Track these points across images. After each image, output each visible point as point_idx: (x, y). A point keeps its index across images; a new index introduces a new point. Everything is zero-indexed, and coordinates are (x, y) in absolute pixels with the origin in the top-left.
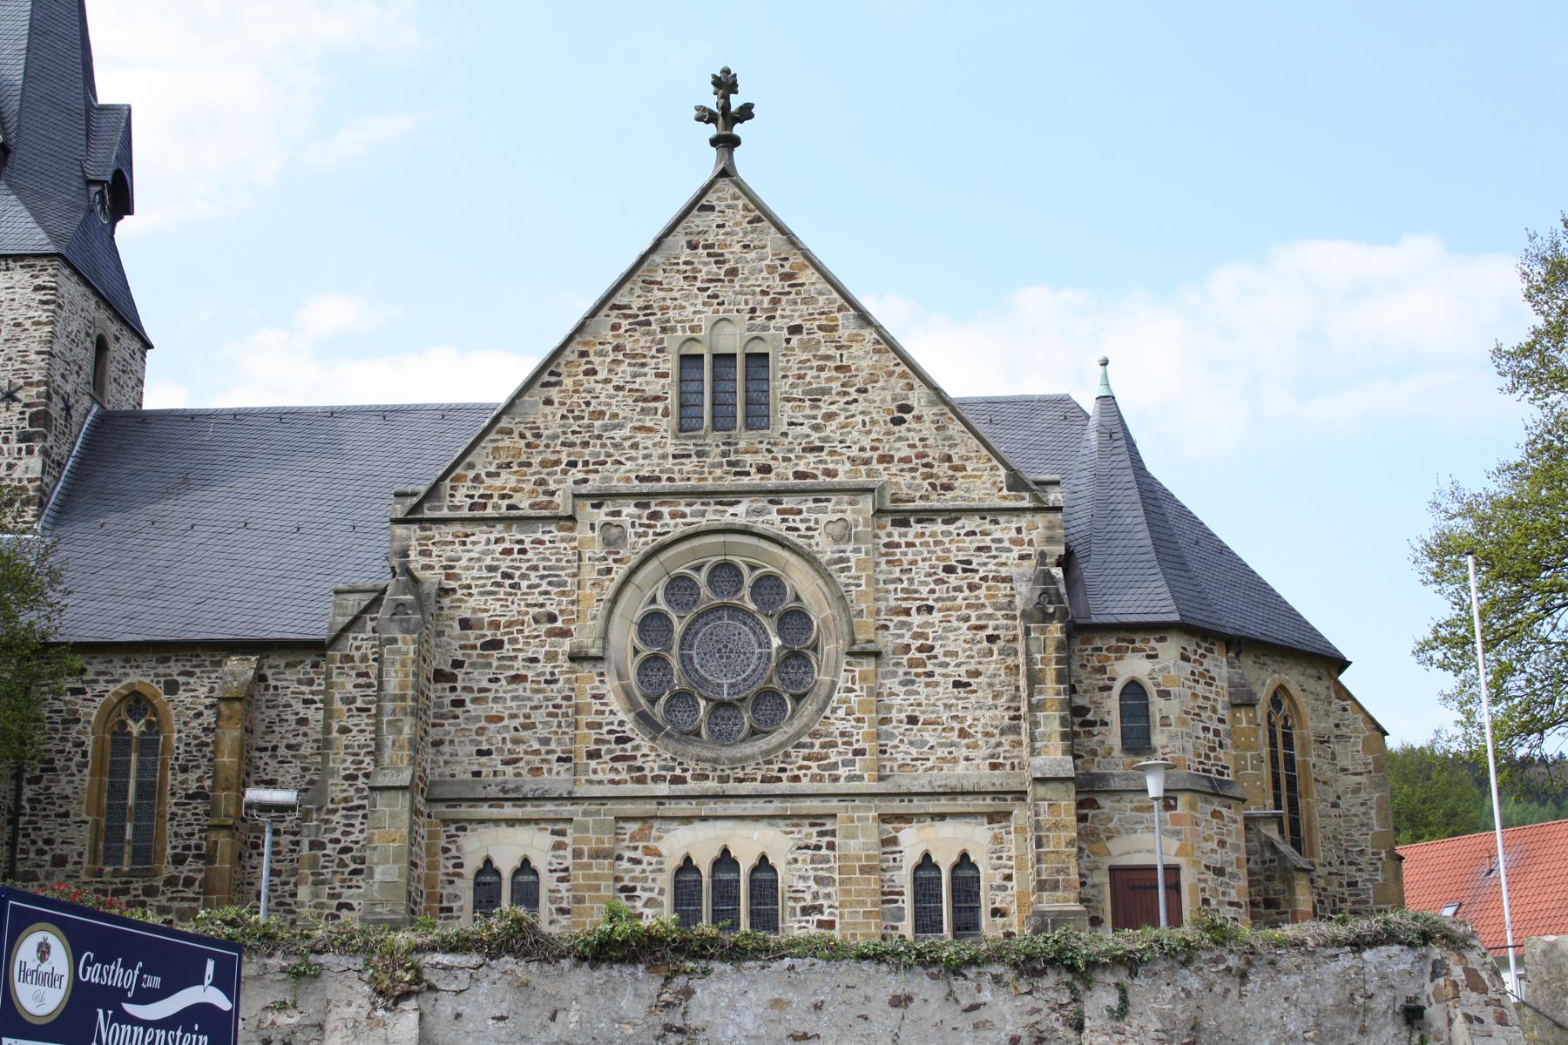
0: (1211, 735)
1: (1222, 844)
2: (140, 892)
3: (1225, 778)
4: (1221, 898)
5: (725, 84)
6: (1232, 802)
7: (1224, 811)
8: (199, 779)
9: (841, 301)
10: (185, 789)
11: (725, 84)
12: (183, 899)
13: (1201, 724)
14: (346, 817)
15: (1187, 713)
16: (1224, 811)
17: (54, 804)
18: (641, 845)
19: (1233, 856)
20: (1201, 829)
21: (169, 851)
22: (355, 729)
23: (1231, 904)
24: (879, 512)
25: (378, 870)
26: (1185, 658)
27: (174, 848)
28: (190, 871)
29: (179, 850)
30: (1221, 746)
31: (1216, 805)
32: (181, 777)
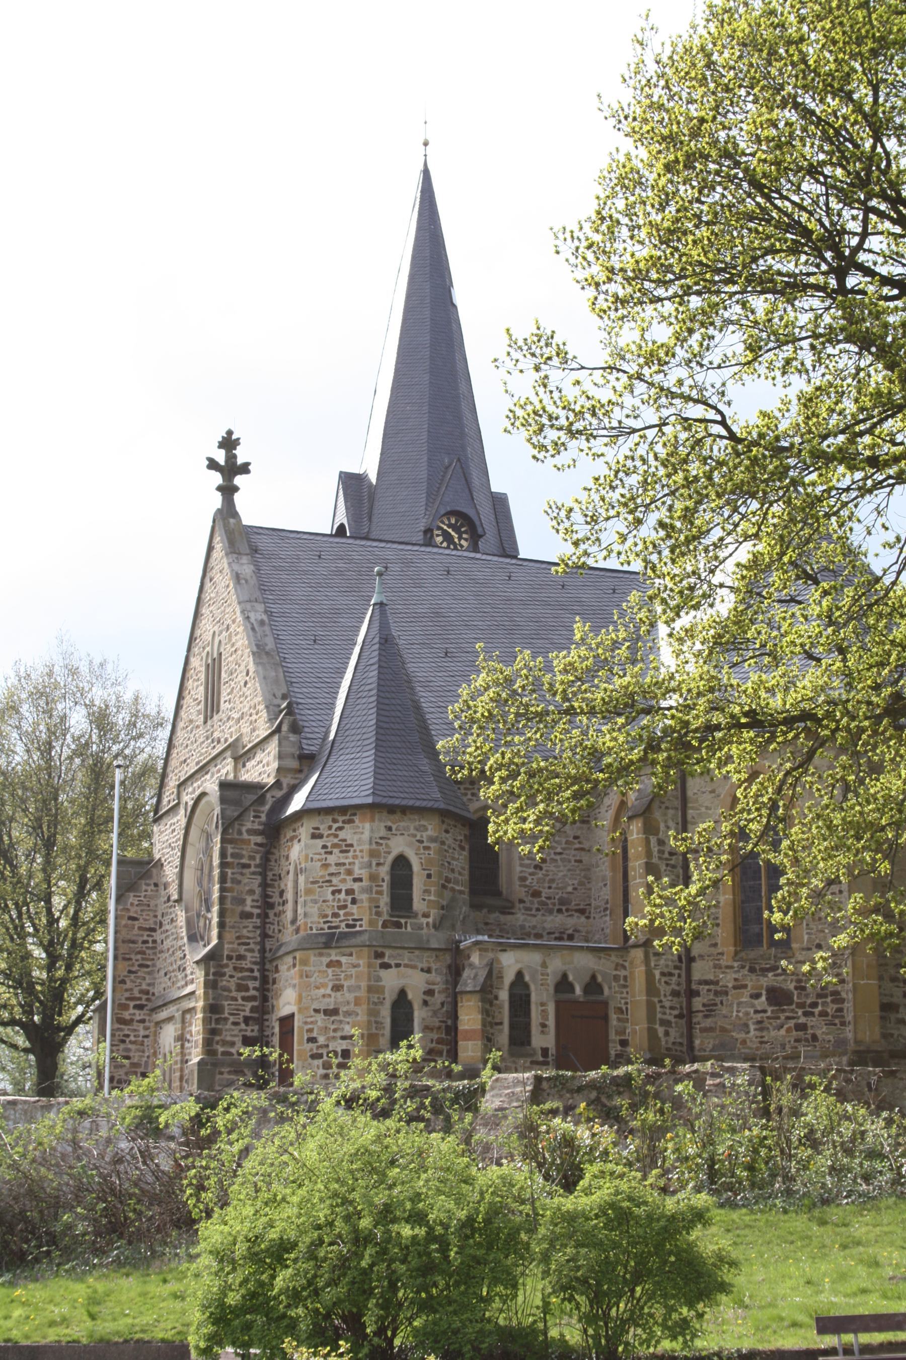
0: (343, 896)
1: (337, 988)
3: (358, 929)
4: (332, 1034)
5: (229, 443)
6: (353, 950)
7: (344, 960)
11: (229, 443)
13: (331, 889)
15: (313, 883)
16: (344, 960)
19: (350, 997)
20: (312, 979)
23: (343, 1038)
24: (236, 759)
26: (314, 836)
30: (354, 901)
31: (334, 955)
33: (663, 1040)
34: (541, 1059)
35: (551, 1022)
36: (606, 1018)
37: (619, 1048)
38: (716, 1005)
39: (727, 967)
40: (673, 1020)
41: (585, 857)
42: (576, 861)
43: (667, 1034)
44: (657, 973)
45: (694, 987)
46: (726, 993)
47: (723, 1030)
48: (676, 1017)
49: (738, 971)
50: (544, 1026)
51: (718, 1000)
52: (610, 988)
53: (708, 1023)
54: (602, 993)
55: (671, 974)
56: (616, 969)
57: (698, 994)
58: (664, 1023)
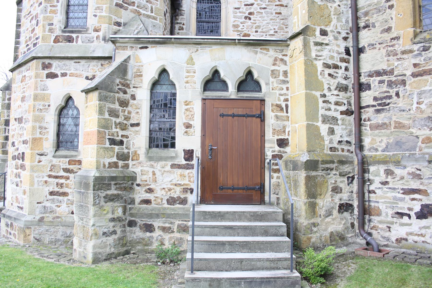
33: (327, 139)
34: (184, 162)
35: (197, 123)
36: (262, 117)
37: (277, 148)
38: (390, 97)
39: (403, 52)
40: (339, 117)
41: (283, 10)
42: (276, 13)
43: (332, 132)
44: (319, 65)
45: (363, 80)
46: (404, 83)
47: (399, 126)
48: (342, 113)
49: (420, 54)
50: (188, 126)
51: (393, 92)
52: (267, 84)
53: (380, 118)
54: (260, 90)
55: (336, 67)
56: (274, 65)
57: (368, 87)
58: (326, 119)
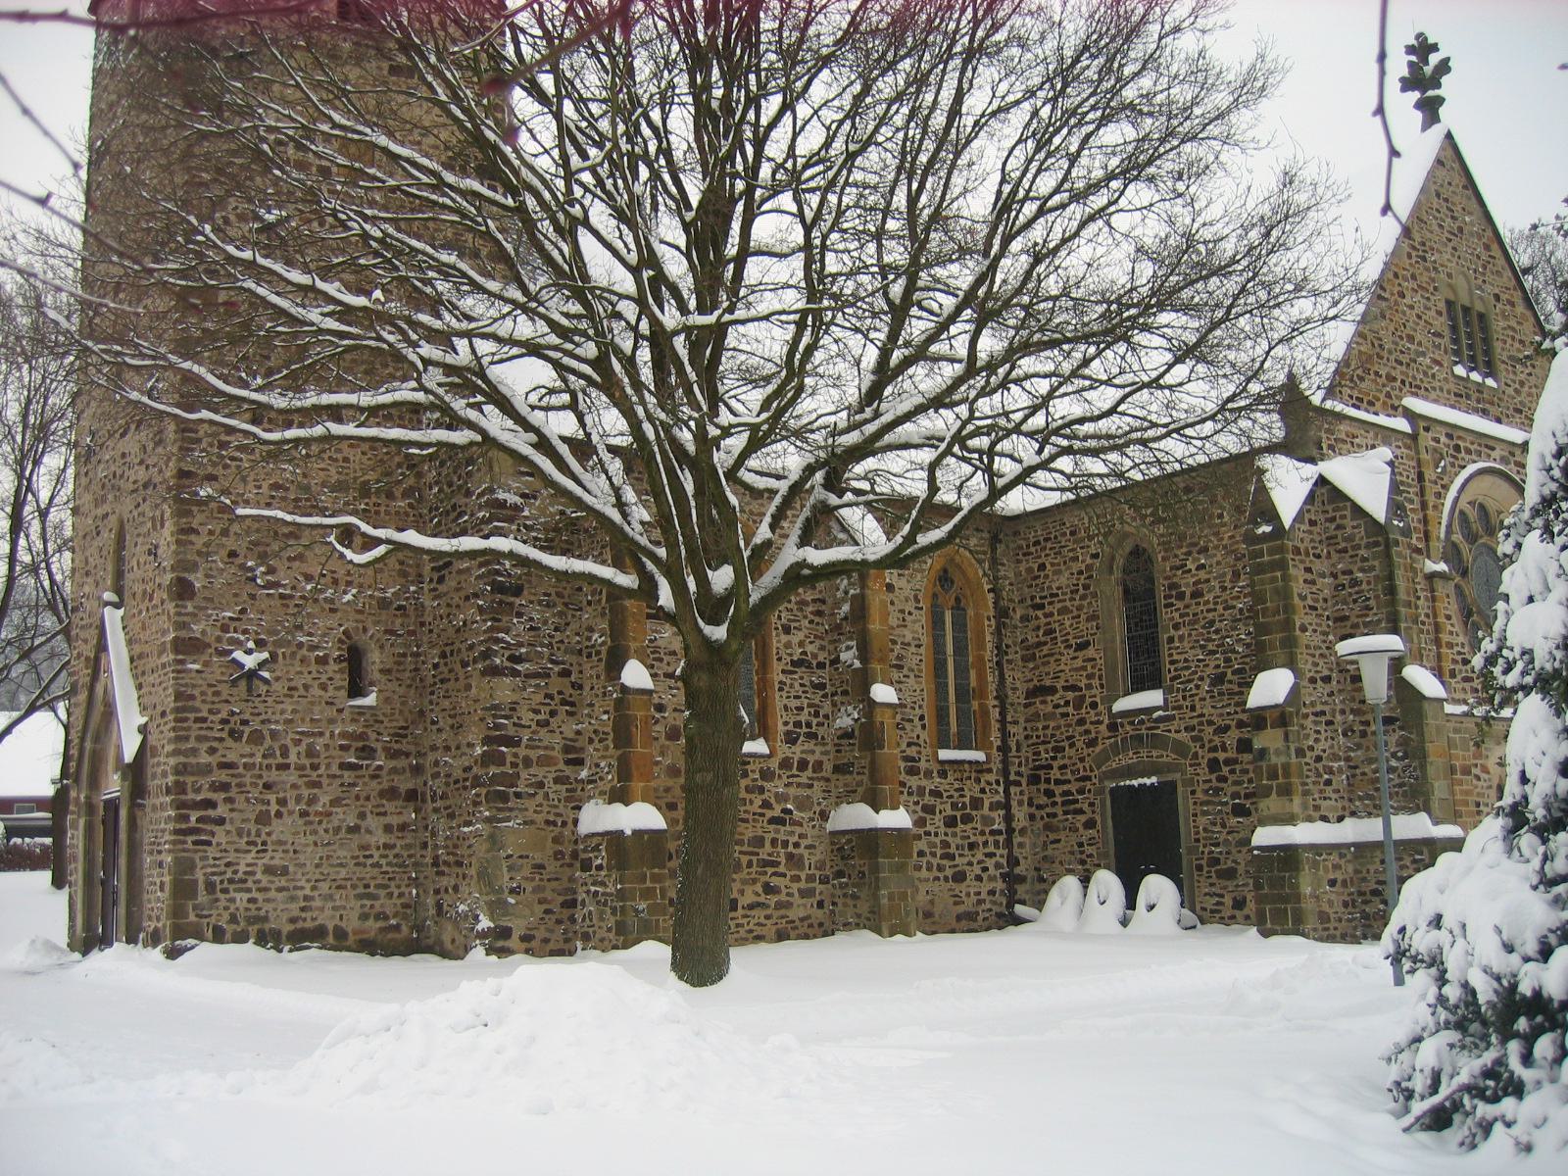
2: (757, 776)
5: (1422, 48)
8: (801, 644)
9: (1514, 282)
10: (791, 655)
12: (799, 785)
14: (1316, 723)
17: (661, 660)
18: (1479, 762)
21: (781, 728)
22: (1310, 628)
25: (1436, 785)
27: (786, 724)
28: (802, 752)
29: (790, 727)
32: (784, 638)
